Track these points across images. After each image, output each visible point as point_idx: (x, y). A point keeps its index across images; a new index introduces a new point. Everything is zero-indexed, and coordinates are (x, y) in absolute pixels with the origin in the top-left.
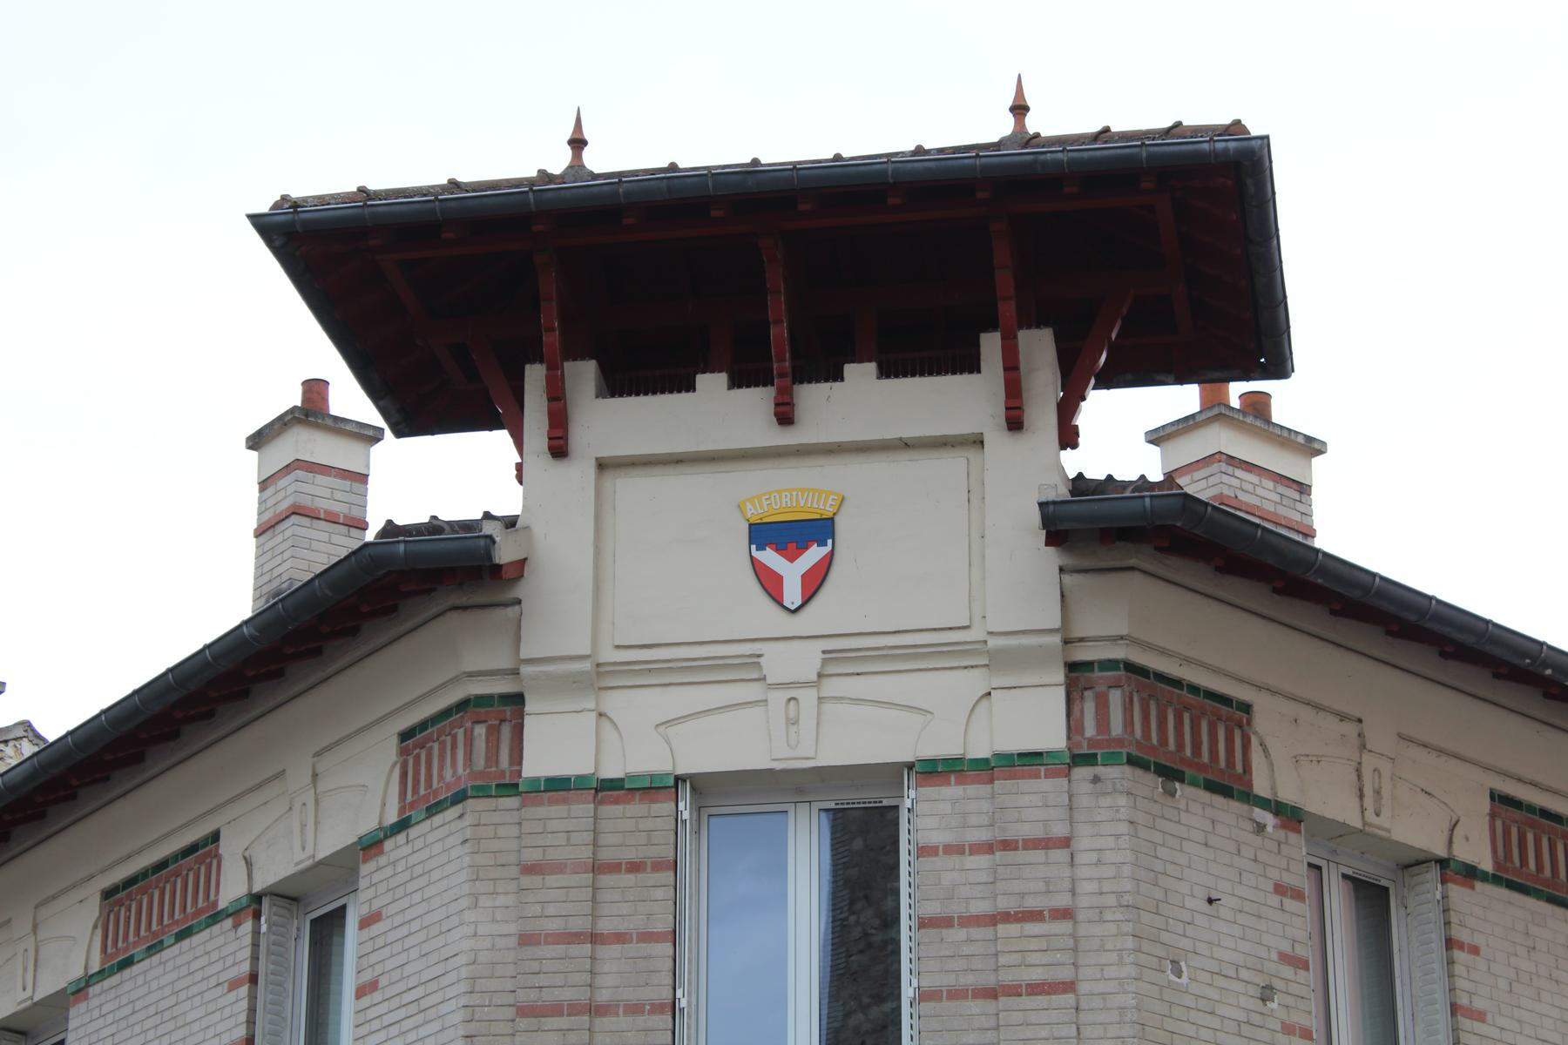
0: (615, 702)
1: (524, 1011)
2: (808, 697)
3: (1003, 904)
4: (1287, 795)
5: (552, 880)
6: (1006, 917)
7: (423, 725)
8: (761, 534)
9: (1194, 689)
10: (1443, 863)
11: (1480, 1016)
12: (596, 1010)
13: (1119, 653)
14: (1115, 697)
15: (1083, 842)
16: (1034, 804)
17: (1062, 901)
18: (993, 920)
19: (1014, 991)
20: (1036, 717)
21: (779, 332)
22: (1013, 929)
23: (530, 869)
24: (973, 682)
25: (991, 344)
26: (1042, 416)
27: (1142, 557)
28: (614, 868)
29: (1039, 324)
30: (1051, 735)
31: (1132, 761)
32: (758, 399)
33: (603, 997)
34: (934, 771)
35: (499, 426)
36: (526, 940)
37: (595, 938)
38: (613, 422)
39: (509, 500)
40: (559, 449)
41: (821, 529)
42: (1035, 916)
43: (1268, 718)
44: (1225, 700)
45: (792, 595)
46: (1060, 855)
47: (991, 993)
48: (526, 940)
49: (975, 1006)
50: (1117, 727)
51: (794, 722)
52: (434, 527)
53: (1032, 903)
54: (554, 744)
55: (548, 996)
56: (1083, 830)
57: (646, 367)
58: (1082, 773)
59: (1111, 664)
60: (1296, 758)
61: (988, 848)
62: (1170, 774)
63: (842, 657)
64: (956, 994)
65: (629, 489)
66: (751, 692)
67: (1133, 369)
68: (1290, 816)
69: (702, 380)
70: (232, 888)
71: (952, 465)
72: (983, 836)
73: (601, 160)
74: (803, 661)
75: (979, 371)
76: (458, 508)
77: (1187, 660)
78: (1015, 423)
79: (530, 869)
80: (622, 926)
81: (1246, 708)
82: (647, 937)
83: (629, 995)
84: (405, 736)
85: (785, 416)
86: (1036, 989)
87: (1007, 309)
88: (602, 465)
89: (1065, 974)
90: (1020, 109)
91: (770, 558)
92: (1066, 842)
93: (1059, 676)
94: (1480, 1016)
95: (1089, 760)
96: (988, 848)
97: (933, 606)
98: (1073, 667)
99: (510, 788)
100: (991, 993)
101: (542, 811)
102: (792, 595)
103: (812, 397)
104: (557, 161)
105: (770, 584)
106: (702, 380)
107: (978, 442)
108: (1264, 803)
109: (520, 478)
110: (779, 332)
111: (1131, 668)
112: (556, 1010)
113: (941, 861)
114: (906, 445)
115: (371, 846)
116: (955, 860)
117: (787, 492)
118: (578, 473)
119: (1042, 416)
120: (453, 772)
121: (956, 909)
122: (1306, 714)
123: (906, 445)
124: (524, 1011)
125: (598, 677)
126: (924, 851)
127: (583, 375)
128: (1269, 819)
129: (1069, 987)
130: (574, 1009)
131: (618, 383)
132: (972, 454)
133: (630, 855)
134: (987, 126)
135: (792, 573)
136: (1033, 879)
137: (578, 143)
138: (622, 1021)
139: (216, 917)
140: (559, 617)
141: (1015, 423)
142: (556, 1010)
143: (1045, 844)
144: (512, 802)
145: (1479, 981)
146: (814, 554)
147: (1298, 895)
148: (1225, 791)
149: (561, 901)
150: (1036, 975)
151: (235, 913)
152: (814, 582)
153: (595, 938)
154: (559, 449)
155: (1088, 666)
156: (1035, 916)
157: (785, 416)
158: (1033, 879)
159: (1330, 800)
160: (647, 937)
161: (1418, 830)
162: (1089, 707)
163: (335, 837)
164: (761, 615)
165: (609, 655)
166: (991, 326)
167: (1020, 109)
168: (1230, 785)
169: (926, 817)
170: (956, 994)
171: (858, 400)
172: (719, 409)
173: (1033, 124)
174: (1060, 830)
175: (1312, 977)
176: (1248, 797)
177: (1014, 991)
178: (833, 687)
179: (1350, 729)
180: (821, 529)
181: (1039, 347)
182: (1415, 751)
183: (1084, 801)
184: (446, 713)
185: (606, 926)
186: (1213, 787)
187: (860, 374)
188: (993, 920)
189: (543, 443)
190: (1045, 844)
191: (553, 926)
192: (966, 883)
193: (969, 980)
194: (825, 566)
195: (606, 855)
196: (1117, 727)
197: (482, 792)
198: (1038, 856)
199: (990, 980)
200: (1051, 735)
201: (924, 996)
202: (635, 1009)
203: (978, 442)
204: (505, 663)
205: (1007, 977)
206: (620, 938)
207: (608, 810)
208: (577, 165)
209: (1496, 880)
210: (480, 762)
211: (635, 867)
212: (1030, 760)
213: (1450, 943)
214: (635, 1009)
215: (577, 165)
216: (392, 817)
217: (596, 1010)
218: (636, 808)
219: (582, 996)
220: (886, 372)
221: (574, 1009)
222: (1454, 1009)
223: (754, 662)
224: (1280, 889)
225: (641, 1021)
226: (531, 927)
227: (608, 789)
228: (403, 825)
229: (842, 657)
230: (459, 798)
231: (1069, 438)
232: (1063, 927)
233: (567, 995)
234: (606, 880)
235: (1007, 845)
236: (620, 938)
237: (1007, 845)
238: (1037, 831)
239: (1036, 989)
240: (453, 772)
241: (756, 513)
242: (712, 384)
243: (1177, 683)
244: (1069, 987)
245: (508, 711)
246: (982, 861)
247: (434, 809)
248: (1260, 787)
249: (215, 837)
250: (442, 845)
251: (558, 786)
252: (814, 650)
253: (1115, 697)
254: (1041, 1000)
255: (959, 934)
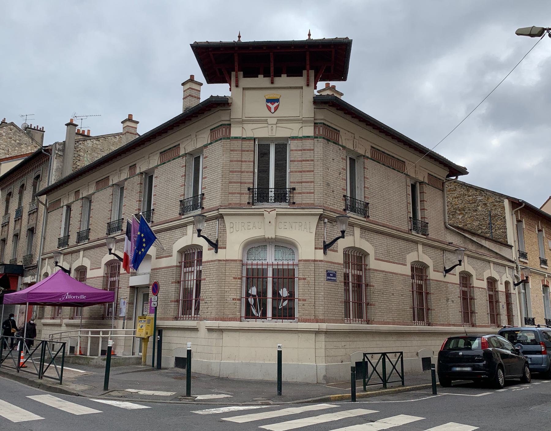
0: (245, 126)
1: (231, 172)
2: (274, 126)
3: (303, 159)
4: (344, 145)
5: (235, 152)
6: (304, 161)
7: (214, 128)
8: (268, 101)
9: (332, 128)
10: (364, 156)
11: (368, 179)
12: (242, 172)
13: (322, 121)
14: (321, 128)
15: (315, 150)
16: (308, 144)
17: (312, 158)
18: (301, 161)
19: (304, 171)
20: (309, 131)
21: (272, 69)
22: (305, 162)
23: (232, 151)
24: (299, 125)
25: (305, 72)
26: (312, 84)
27: (326, 106)
28: (244, 151)
29: (312, 69)
30: (311, 134)
31: (323, 138)
32: (268, 80)
33: (243, 170)
34: (293, 138)
35: (227, 83)
36: (231, 161)
37: (242, 161)
38: (246, 82)
39: (228, 94)
40: (237, 86)
41: (277, 100)
42: (308, 161)
43: (342, 132)
44: (336, 130)
45: (273, 110)
46: (312, 152)
47: (301, 172)
48: (231, 161)
49: (299, 174)
50: (321, 133)
51: (272, 130)
52: (218, 97)
53: (307, 159)
54: (236, 132)
55: (234, 170)
56: (316, 148)
57: (250, 73)
58: (316, 139)
59: (321, 123)
60: (345, 140)
61: (301, 150)
62: (328, 140)
63: (280, 120)
64: (296, 172)
65: (247, 92)
66: (266, 125)
67: (323, 79)
68: (344, 148)
69: (259, 76)
70: (182, 152)
71: (298, 91)
72: (301, 148)
73: (243, 40)
74: (274, 121)
75: (302, 76)
76: (221, 95)
77: (331, 123)
78: (308, 85)
79: (232, 151)
80: (246, 160)
81: (339, 131)
82: (249, 161)
83: (246, 170)
84: (211, 130)
85: (272, 83)
86: (308, 171)
87: (308, 67)
88: (244, 89)
89: (313, 169)
90: (309, 35)
91: (269, 104)
92: (313, 150)
93: (313, 125)
94: (368, 179)
95: (317, 138)
96: (301, 150)
97: (294, 113)
98: (315, 123)
99: (229, 138)
100: (301, 172)
101: (233, 142)
102: (273, 110)
103: (277, 79)
104: (236, 40)
105: (269, 109)
106: (259, 76)
107: (302, 88)
108: (341, 146)
109: (230, 91)
110: (272, 69)
111: (324, 124)
112: (236, 172)
113: (294, 152)
114: (291, 88)
115: (206, 146)
116: (296, 152)
117: (272, 94)
118: (240, 90)
119: (312, 84)
120: (220, 135)
121: (296, 159)
122: (347, 132)
123: (291, 88)
124: (231, 172)
125: (242, 122)
126: (291, 150)
127: (241, 74)
128: (341, 148)
129: (313, 171)
130: (238, 172)
131: (247, 75)
132: (301, 90)
133: (247, 149)
134: (305, 38)
135: (273, 107)
136: (308, 155)
137: (239, 37)
138: (245, 174)
139: (179, 157)
140: (237, 112)
141: (308, 85)
142: (236, 172)
143: (310, 150)
144: (229, 140)
145: (368, 174)
146: (276, 104)
147: (344, 159)
148: (336, 144)
149: (236, 156)
150: (308, 169)
151: (183, 156)
152: (276, 109)
153: (242, 161)
154: (237, 86)
155: (317, 123)
156: (308, 161)
157: (272, 83)
158: (308, 155)
159: (350, 146)
160: (249, 161)
161: (361, 152)
162: (317, 129)
163: (199, 145)
164: (268, 114)
165: (244, 119)
166: (305, 69)
167: (309, 35)
168: (336, 143)
169: (292, 145)
170: (296, 172)
171: (283, 80)
172: (262, 81)
173: (311, 38)
174: (312, 148)
175: (345, 171)
176: (338, 144)
177: (304, 171)
178: (278, 125)
179: (353, 135)
180: (277, 100)
181: (312, 73)
182: (361, 139)
183: (316, 144)
184: (218, 126)
185: (243, 160)
186: (334, 143)
187: (284, 76)
188: (301, 161)
189: (235, 85)
190: (310, 150)
191: (236, 159)
192: (297, 155)
193: (298, 170)
194: (278, 106)
195: (243, 149)
196: (321, 133)
197: (224, 139)
198: (309, 152)
199: (301, 170)
200: (311, 134)
201: (291, 172)
202: (247, 172)
203: (302, 88)
204: (228, 119)
205: (304, 169)
206: (245, 161)
207: (243, 142)
208: (239, 40)
209: (371, 159)
210: (224, 134)
211: (248, 151)
212: (308, 137)
213: (364, 168)
214: (247, 172)
215: (239, 40)
216: (209, 142)
217: (242, 172)
218: (248, 142)
219: (240, 170)
220: (287, 76)
221: (238, 172)
222: (364, 177)
223: (266, 121)
224: (342, 158)
225: (248, 174)
226: (232, 159)
227: (244, 139)
228: (211, 143)
229: (280, 120)
230: (221, 139)
231: (315, 88)
232: (313, 162)
233: (237, 169)
234: (243, 153)
235: (304, 150)
236: (245, 161)
237: (304, 150)
238: (309, 148)
239: (308, 171)
240: (220, 135)
241: (267, 97)
242: (261, 76)
243: (330, 127)
244: (313, 171)
245: (228, 126)
246: (300, 152)
247: (216, 141)
248: (340, 143)
249: (179, 145)
250: (218, 147)
251: (236, 138)
252: (276, 119)
253: (321, 128)
254: (309, 173)
255: (296, 163)
